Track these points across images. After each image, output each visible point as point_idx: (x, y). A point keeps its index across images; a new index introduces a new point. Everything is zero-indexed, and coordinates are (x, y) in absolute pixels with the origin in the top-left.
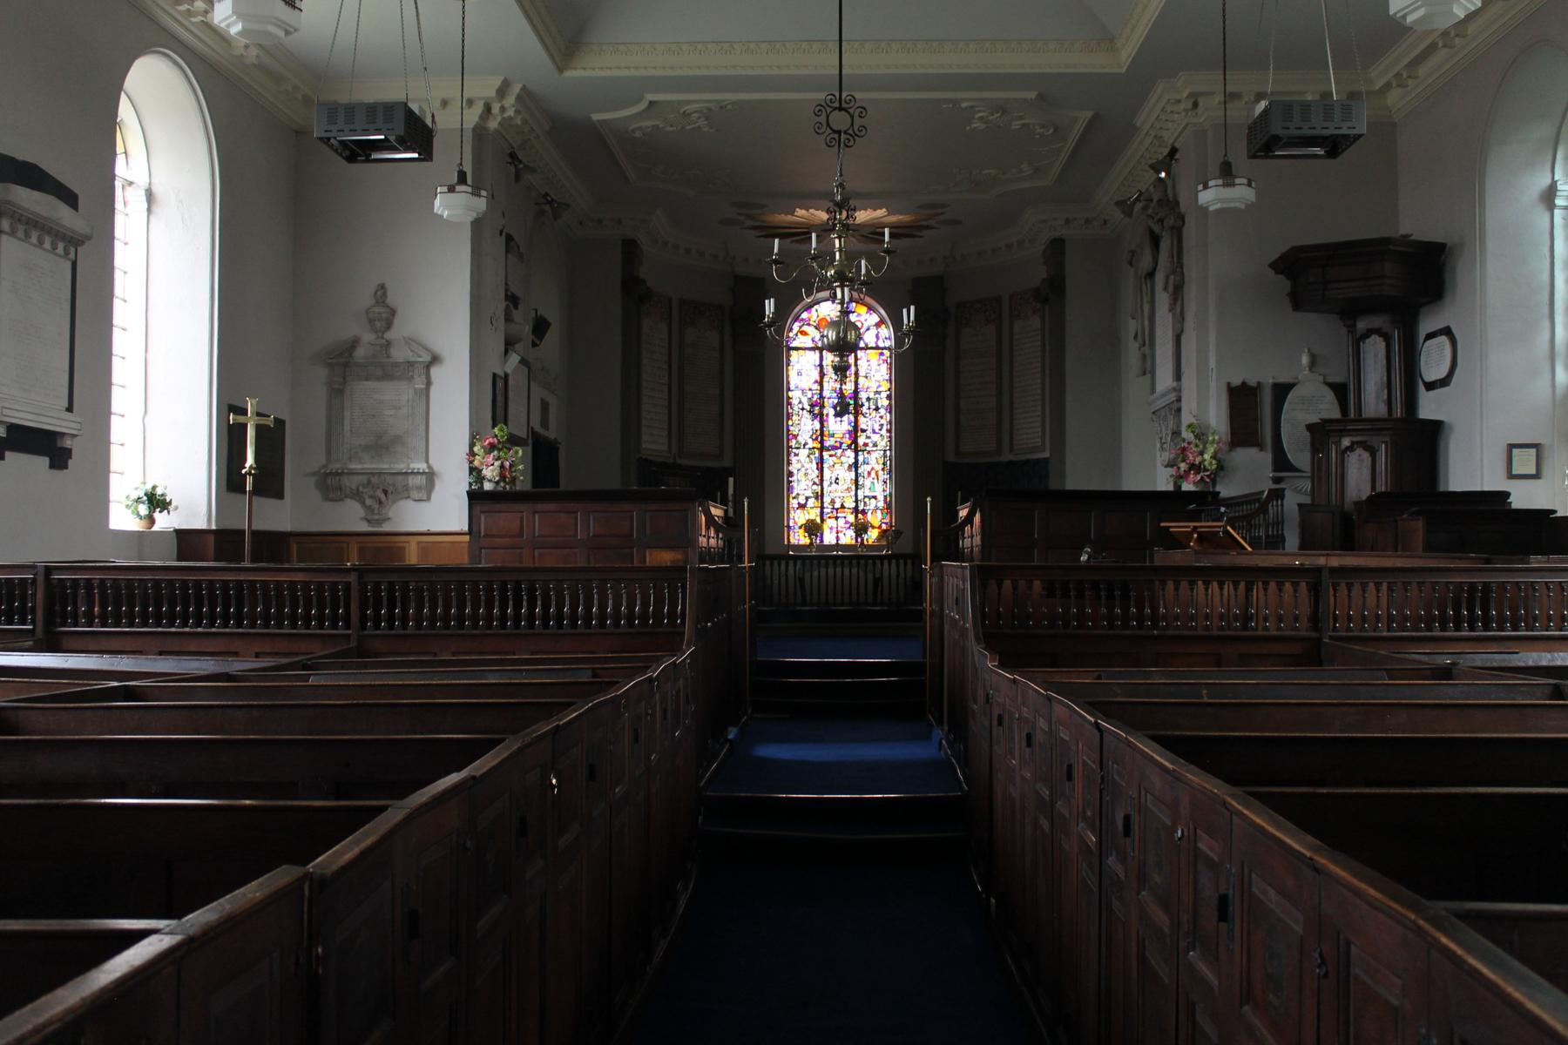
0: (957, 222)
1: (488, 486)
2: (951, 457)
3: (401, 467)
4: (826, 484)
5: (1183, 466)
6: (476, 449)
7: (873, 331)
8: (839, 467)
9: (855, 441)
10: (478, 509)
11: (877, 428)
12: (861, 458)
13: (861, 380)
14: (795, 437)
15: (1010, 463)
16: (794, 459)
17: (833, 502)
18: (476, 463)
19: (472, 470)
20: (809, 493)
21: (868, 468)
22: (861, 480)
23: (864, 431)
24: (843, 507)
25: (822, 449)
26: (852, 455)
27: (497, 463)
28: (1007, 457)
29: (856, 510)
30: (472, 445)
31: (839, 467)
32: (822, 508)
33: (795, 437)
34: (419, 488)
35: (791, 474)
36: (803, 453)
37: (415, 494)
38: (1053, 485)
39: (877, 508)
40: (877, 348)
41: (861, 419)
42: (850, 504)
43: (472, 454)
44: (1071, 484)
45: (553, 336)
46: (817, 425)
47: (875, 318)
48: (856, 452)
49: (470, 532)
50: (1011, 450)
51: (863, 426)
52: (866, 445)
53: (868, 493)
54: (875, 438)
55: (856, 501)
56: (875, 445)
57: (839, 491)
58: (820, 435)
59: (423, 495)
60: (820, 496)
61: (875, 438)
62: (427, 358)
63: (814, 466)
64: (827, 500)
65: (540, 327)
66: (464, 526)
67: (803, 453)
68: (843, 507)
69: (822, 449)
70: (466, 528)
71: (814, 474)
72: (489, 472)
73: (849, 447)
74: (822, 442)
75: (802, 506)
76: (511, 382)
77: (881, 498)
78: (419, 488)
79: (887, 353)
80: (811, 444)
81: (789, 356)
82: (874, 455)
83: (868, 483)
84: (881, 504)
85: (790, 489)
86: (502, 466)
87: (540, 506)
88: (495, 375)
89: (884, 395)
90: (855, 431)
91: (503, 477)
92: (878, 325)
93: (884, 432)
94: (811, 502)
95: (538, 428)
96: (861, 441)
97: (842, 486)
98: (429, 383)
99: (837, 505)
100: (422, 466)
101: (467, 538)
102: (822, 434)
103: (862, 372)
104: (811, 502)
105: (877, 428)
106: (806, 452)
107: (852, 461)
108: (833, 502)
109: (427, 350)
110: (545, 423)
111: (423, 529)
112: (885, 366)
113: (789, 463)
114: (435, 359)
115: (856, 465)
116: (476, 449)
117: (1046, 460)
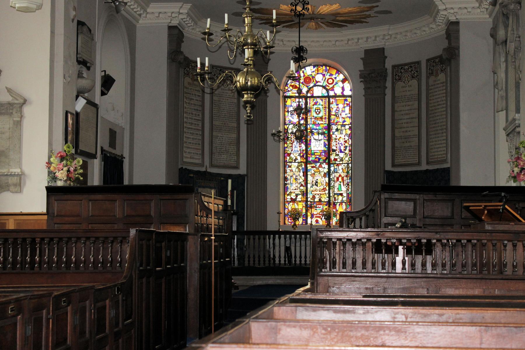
0: (390, 12)
1: (60, 184)
2: (388, 167)
3: (5, 171)
4: (309, 186)
5: (516, 170)
6: (52, 160)
7: (340, 84)
8: (318, 176)
9: (328, 158)
10: (53, 198)
11: (342, 148)
12: (332, 169)
13: (332, 117)
14: (289, 155)
15: (427, 171)
16: (288, 170)
17: (314, 197)
18: (52, 168)
19: (50, 173)
20: (298, 192)
21: (337, 175)
22: (332, 183)
23: (334, 151)
24: (320, 200)
25: (306, 163)
26: (327, 167)
27: (65, 169)
28: (424, 167)
29: (329, 203)
30: (50, 157)
31: (318, 176)
32: (307, 201)
33: (289, 155)
34: (15, 185)
35: (286, 179)
36: (294, 165)
37: (12, 188)
38: (453, 183)
39: (341, 203)
40: (343, 96)
41: (333, 143)
42: (325, 199)
43: (49, 163)
44: (464, 183)
45: (118, 90)
46: (303, 147)
47: (341, 77)
48: (329, 164)
49: (48, 213)
50: (428, 163)
51: (334, 148)
52: (335, 160)
53: (336, 191)
54: (342, 155)
55: (329, 197)
56: (342, 160)
57: (318, 191)
58: (306, 154)
59: (18, 188)
60: (305, 194)
62: (22, 101)
63: (302, 174)
64: (310, 196)
65: (108, 82)
66: (43, 209)
67: (294, 165)
68: (320, 200)
69: (306, 163)
70: (45, 211)
71: (302, 179)
72: (59, 174)
73: (324, 161)
74: (307, 158)
75: (293, 201)
76: (81, 117)
77: (345, 195)
78: (15, 185)
79: (349, 99)
80: (299, 159)
81: (285, 102)
82: (340, 167)
83: (337, 185)
84: (345, 199)
85: (286, 189)
86: (68, 171)
87: (93, 197)
88: (67, 113)
89: (347, 127)
90: (329, 151)
91: (69, 178)
92: (343, 81)
93: (347, 151)
94: (299, 198)
95: (107, 148)
96: (333, 157)
98: (22, 117)
99: (317, 200)
100: (17, 171)
101: (46, 217)
102: (307, 153)
103: (333, 113)
104: (299, 198)
105: (342, 148)
106: (296, 164)
107: (326, 170)
108: (314, 197)
109: (21, 96)
110: (113, 144)
111: (17, 211)
112: (347, 109)
113: (285, 172)
114: (25, 101)
115: (329, 174)
116: (52, 160)
117: (449, 168)
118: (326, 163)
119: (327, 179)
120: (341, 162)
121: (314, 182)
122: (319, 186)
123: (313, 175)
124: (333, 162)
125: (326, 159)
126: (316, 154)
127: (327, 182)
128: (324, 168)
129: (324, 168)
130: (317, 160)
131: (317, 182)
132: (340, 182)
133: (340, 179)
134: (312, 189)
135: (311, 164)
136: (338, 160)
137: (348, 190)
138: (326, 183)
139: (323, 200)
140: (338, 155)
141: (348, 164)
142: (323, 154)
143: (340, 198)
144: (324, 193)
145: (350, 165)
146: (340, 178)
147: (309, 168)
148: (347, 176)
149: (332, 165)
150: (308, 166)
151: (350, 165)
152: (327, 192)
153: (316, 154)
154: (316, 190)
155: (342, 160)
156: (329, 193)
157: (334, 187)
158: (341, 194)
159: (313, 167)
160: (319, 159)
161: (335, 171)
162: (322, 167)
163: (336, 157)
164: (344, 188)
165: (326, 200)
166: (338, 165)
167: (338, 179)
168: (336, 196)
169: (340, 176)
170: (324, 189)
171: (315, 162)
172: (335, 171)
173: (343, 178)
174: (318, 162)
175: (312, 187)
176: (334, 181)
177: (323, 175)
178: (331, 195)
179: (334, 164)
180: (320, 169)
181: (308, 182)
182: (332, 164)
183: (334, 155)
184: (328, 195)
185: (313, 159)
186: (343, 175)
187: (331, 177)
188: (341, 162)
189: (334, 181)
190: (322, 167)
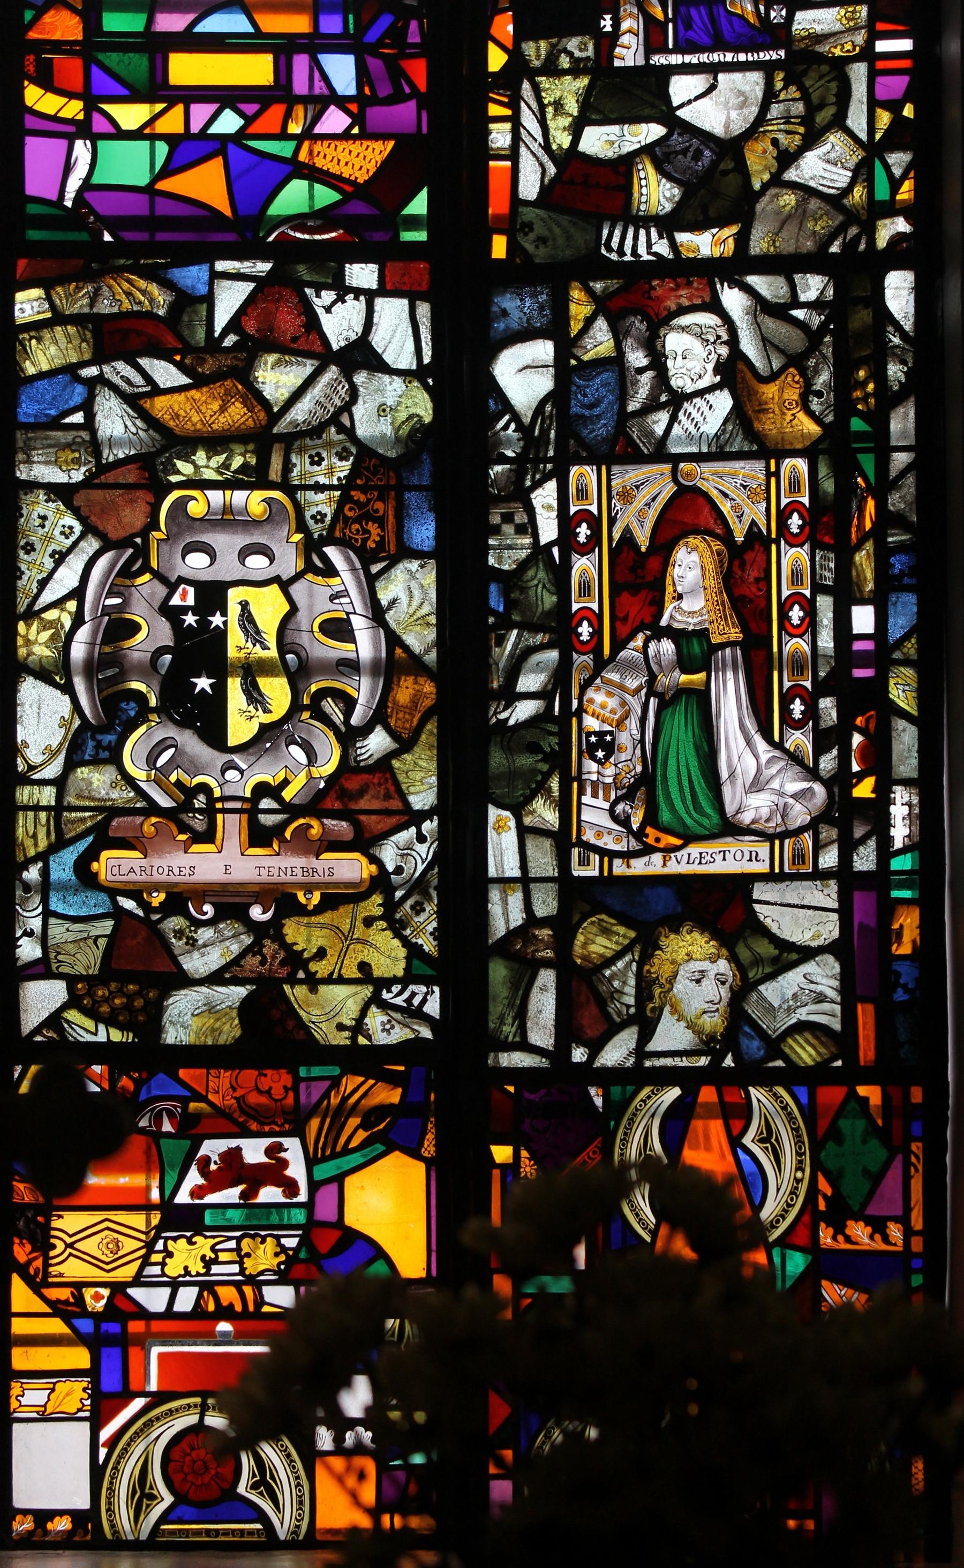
9: (446, 152)
12: (523, 375)
17: (137, 967)
24: (270, 1032)
26: (397, 331)
55: (463, 958)
61: (716, 102)
68: (270, 1032)
73: (363, 220)
77: (802, 915)
82: (689, 353)
84: (806, 993)
97: (266, 746)
107: (389, 408)
108: (137, 967)
115: (447, 477)
118: (384, 253)
119: (411, 591)
120: (704, 243)
121: (151, 636)
122: (241, 725)
123: (128, 498)
124: (554, 240)
125: (391, 183)
126: (185, 69)
127: (420, 639)
128: (361, 356)
129: (361, 356)
130: (206, 184)
131: (199, 649)
132: (696, 650)
133: (690, 567)
134: (98, 781)
135: (91, 265)
136: (656, 192)
137: (846, 816)
138: (395, 663)
139: (330, 1010)
140: (628, 94)
141: (857, 275)
142: (341, 71)
143: (697, 976)
144: (350, 868)
145: (899, 292)
146: (690, 567)
147: (42, 356)
148: (827, 524)
149: (514, 306)
150: (28, 304)
151: (899, 292)
152: (407, 853)
153: (185, 69)
154: (192, 816)
155: (715, 179)
156: (460, 874)
157: (555, 748)
158: (722, 908)
159: (116, 338)
160: (257, 178)
161: (594, 424)
162: (308, 343)
163: (598, 141)
164: (762, 778)
165: (383, 1030)
166: (642, 299)
167: (639, 577)
168: (595, 942)
169: (688, 513)
170: (354, 803)
171: (160, 234)
172: (594, 424)
173: (740, 565)
174: (242, 230)
175: (91, 742)
176: (560, 629)
177: (321, 504)
178: (505, 913)
179: (553, 278)
180: (276, 379)
181: (36, 642)
182: (519, 272)
183: (569, 91)
184: (425, 928)
185: (129, 165)
186: (738, 493)
187: (506, 553)
188: (704, 243)
189: (560, 629)
190: (308, 343)
